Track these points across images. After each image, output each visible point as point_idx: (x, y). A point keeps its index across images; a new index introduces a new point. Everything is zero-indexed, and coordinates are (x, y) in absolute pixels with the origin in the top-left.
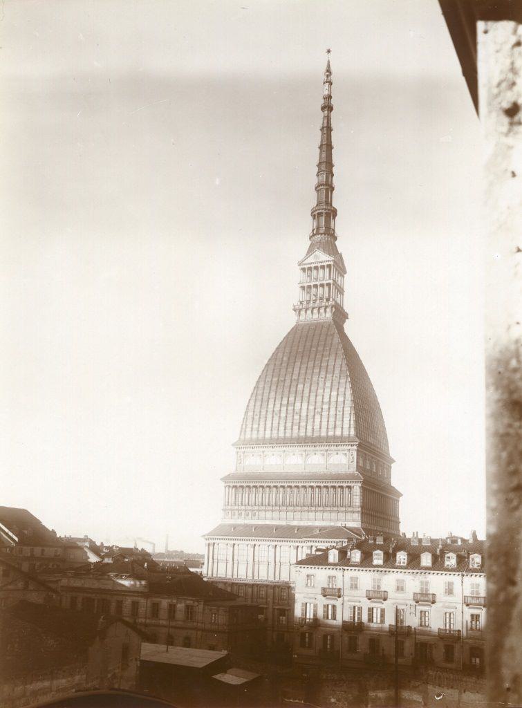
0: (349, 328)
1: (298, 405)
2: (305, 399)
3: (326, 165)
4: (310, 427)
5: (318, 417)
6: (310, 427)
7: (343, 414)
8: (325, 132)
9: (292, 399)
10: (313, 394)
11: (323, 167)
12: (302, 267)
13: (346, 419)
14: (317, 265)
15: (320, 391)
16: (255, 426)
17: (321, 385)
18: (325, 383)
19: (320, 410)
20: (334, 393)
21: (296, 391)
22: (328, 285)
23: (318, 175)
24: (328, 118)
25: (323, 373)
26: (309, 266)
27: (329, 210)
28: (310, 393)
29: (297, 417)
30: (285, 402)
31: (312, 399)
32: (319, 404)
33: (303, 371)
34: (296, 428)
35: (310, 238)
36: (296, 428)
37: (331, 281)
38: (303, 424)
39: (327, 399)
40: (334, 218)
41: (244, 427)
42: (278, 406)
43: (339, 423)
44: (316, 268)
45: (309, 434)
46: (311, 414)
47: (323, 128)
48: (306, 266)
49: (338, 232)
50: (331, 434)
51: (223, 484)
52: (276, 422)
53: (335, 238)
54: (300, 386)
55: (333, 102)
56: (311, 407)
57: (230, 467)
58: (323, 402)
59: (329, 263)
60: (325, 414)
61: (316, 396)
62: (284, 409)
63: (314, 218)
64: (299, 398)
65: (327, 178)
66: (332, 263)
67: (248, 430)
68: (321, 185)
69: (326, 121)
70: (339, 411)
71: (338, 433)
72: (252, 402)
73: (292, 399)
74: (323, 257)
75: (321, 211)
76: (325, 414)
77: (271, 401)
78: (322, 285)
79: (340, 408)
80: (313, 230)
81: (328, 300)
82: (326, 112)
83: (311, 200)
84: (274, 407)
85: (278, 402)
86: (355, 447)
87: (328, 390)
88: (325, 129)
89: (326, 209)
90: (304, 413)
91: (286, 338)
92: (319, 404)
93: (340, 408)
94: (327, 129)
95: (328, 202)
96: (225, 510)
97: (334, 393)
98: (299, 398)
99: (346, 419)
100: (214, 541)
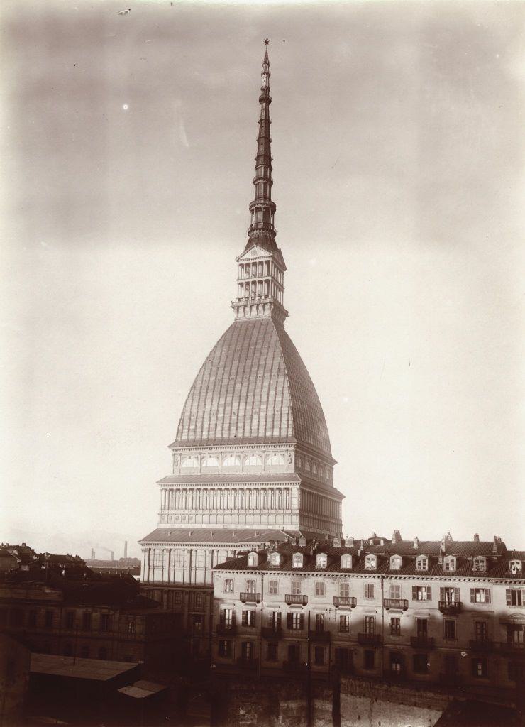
0: (289, 326)
1: (235, 405)
2: (243, 398)
3: (265, 159)
4: (247, 428)
5: (255, 417)
6: (247, 428)
7: (281, 414)
8: (263, 124)
9: (229, 399)
10: (251, 394)
11: (262, 160)
12: (240, 263)
13: (284, 420)
14: (255, 261)
15: (258, 391)
16: (192, 427)
17: (259, 384)
18: (263, 382)
19: (257, 410)
20: (272, 393)
21: (234, 390)
22: (267, 281)
23: (256, 169)
24: (266, 111)
25: (261, 372)
26: (248, 262)
27: (267, 205)
28: (248, 392)
29: (234, 417)
30: (222, 402)
31: (250, 399)
32: (257, 403)
33: (241, 370)
34: (233, 428)
35: (249, 233)
36: (233, 428)
37: (270, 278)
38: (240, 425)
39: (264, 399)
40: (273, 213)
41: (181, 427)
42: (215, 405)
43: (277, 423)
44: (255, 264)
45: (247, 434)
46: (249, 414)
47: (261, 120)
48: (245, 262)
49: (277, 227)
50: (268, 434)
51: (159, 488)
52: (213, 423)
53: (274, 234)
54: (238, 386)
55: (271, 94)
56: (249, 407)
57: (166, 470)
58: (260, 401)
59: (268, 259)
60: (263, 414)
61: (254, 395)
62: (221, 409)
63: (253, 213)
64: (236, 398)
65: (266, 172)
66: (270, 259)
67: (185, 431)
68: (260, 179)
69: (264, 114)
70: (278, 411)
71: (276, 433)
72: (190, 401)
73: (229, 399)
74: (261, 253)
75: (259, 206)
76: (263, 414)
77: (209, 401)
78: (261, 282)
79: (278, 408)
80: (252, 225)
81: (266, 297)
82: (264, 104)
83: (250, 194)
84: (211, 407)
85: (215, 402)
86: (293, 448)
87: (265, 390)
88: (263, 121)
89: (264, 204)
90: (241, 414)
91: (224, 336)
92: (257, 403)
93: (278, 408)
94: (265, 123)
95: (267, 197)
96: (161, 514)
97: (272, 393)
98: (236, 398)
99: (284, 420)
100: (150, 547)
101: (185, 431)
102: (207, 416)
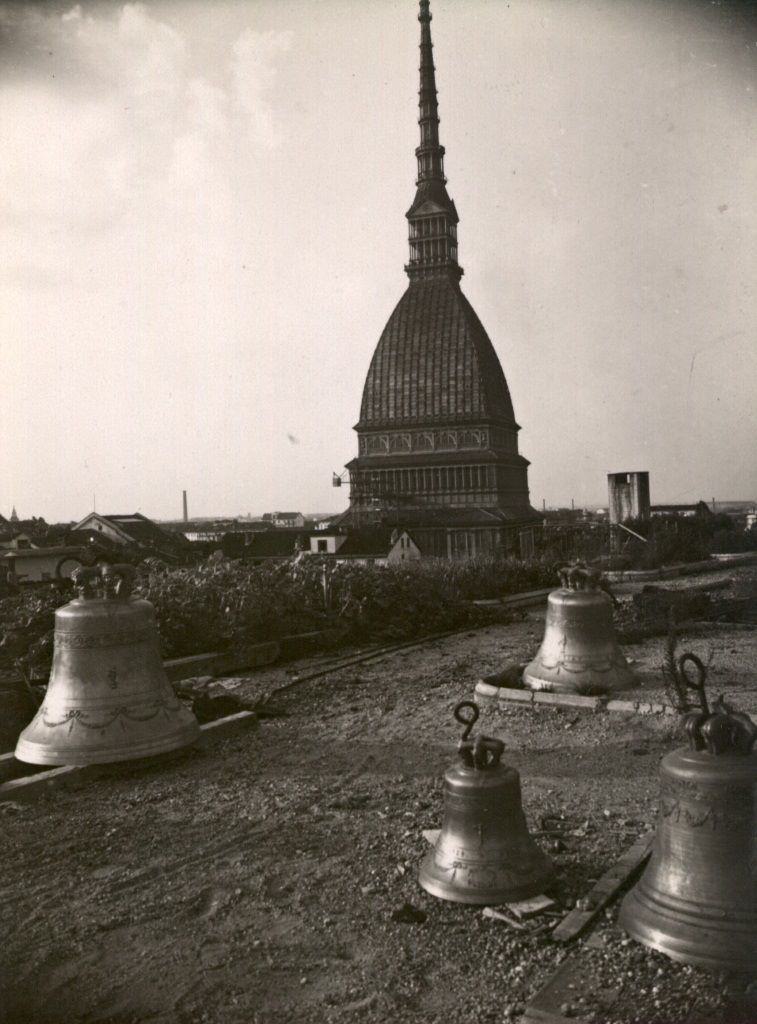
17: (445, 358)
20: (460, 367)
30: (407, 379)
36: (422, 406)
42: (400, 383)
52: (399, 401)
64: (422, 375)
67: (370, 410)
72: (371, 379)
85: (399, 379)
87: (453, 364)
99: (476, 395)
101: (370, 410)
102: (392, 395)
